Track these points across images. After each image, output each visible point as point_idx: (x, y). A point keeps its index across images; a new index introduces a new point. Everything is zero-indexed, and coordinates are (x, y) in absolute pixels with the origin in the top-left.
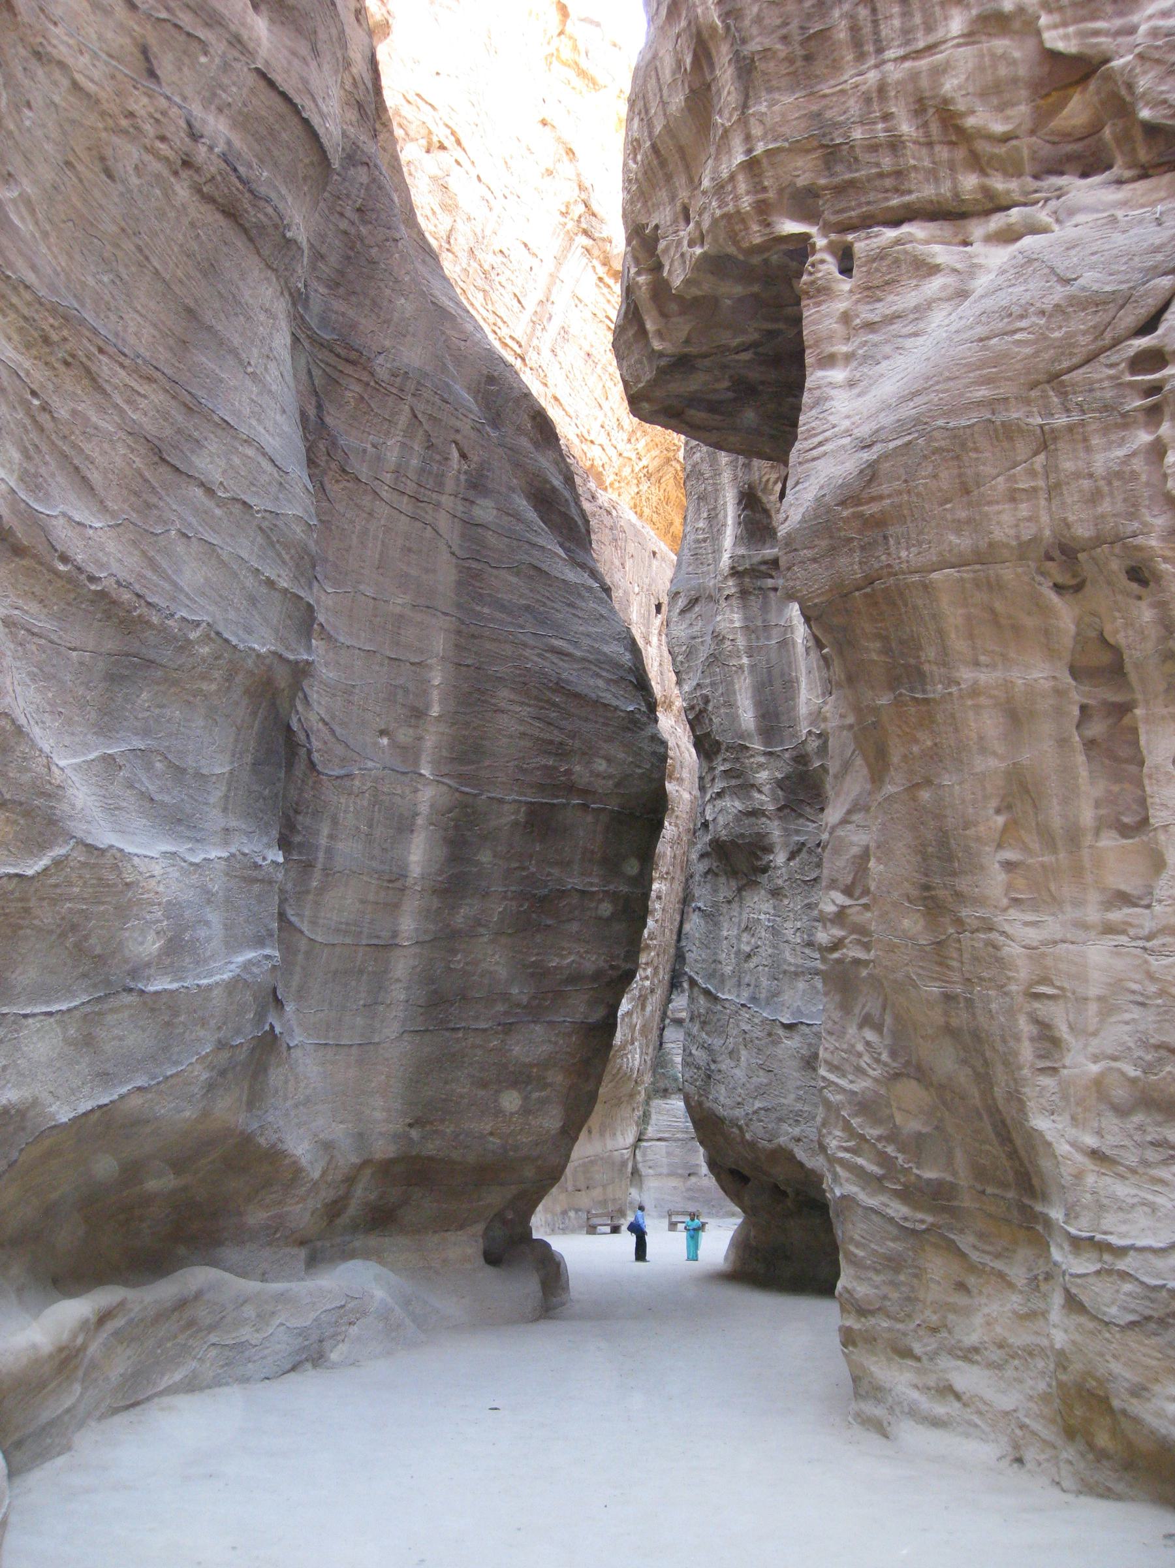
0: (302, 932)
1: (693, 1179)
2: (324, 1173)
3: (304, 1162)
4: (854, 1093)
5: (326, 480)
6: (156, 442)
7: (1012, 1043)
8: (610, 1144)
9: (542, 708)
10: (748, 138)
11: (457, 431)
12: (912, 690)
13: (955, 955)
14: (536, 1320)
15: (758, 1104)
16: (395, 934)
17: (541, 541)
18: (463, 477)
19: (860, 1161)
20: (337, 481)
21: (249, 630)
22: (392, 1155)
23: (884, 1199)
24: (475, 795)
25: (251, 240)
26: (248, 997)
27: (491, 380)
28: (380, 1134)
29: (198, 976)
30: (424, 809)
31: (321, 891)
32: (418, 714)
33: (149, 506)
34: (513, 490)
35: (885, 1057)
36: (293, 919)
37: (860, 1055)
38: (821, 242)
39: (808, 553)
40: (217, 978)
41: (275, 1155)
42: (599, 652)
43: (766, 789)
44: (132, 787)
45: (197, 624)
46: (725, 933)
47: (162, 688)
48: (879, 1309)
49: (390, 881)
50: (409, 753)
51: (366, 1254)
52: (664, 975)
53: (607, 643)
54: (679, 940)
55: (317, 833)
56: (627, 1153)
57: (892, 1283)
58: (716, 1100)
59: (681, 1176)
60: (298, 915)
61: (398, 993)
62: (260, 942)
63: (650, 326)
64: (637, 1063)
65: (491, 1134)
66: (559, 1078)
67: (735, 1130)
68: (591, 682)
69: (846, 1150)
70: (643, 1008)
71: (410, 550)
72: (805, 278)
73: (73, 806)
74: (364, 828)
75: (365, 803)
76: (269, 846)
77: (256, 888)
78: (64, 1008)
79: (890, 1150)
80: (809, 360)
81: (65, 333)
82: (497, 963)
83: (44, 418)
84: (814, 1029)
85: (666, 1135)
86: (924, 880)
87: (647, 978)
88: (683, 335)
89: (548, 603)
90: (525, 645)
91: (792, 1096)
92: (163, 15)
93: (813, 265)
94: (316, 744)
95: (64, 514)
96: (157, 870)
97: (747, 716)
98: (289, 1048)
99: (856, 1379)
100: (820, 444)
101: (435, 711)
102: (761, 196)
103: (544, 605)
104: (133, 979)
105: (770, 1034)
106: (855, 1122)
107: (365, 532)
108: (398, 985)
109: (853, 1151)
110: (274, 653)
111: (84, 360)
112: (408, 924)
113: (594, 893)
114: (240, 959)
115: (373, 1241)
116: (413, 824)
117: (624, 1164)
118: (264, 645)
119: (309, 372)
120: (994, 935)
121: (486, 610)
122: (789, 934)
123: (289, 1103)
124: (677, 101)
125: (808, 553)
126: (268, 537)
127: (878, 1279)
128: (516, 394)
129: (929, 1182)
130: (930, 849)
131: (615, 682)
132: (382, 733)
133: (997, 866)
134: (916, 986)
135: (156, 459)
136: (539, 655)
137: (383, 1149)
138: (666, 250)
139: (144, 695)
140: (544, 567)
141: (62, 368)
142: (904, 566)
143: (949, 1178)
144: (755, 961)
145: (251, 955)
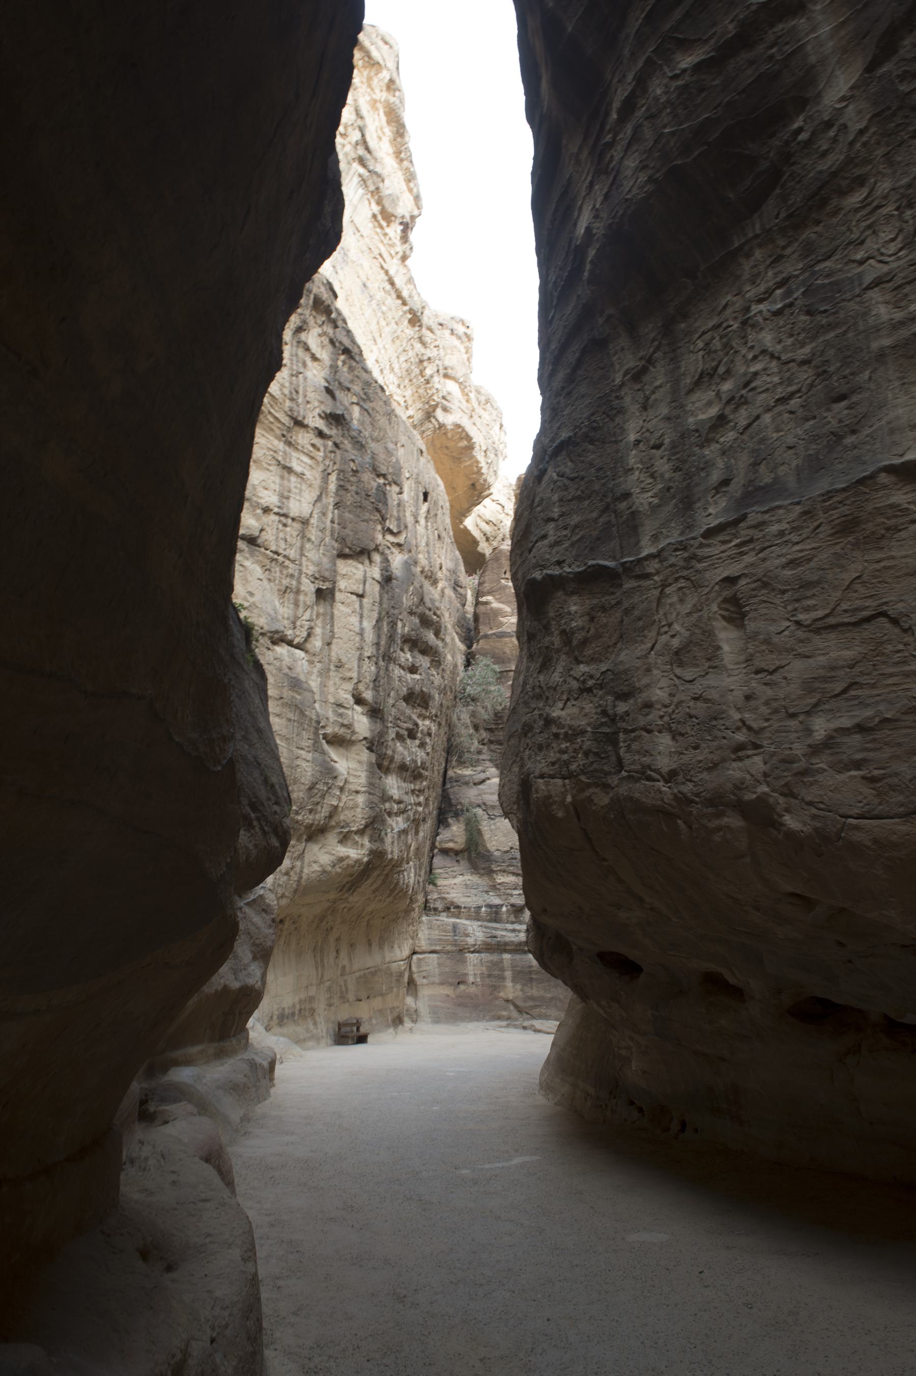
1: (462, 987)
8: (388, 956)
15: (821, 727)
46: (632, 437)
52: (433, 807)
54: (444, 783)
58: (645, 773)
59: (451, 984)
64: (412, 881)
67: (733, 821)
70: (417, 833)
85: (438, 948)
87: (419, 804)
117: (401, 975)
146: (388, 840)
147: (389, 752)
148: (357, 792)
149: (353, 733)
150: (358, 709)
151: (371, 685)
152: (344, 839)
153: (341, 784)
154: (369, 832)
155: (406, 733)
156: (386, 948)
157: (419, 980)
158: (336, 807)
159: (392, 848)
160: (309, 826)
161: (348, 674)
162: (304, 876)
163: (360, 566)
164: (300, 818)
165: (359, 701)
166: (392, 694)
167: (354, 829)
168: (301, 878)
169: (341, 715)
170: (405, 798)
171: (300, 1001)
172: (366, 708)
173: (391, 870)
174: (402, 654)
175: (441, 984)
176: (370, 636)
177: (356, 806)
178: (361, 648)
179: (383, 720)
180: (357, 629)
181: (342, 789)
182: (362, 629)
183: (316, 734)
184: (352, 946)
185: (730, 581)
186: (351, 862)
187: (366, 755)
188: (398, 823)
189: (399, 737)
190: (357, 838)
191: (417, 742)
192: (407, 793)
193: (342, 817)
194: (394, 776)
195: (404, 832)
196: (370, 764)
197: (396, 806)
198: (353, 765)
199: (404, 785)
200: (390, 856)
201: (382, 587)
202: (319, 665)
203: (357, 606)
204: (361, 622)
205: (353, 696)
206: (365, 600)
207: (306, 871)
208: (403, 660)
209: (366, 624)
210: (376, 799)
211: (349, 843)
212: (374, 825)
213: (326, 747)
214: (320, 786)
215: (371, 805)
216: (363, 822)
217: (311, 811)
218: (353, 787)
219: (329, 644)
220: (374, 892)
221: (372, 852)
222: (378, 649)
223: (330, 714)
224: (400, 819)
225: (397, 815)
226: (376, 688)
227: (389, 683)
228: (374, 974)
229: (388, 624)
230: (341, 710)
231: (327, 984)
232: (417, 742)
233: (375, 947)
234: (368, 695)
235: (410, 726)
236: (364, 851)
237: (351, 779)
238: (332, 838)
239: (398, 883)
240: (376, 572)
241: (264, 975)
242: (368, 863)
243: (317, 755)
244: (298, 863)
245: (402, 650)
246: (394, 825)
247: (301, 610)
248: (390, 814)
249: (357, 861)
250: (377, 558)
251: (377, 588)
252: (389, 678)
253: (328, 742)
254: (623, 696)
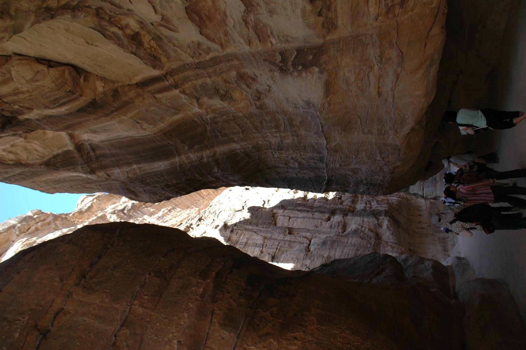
1: (437, 179)
8: (424, 208)
15: (379, 158)
43: (199, 154)
46: (295, 175)
56: (428, 202)
59: (436, 183)
64: (396, 198)
84: (324, 122)
85: (422, 188)
91: (369, 136)
97: (161, 165)
105: (336, 151)
117: (431, 203)
122: (278, 140)
144: (300, 160)
146: (381, 209)
147: (348, 207)
148: (363, 221)
149: (341, 222)
150: (332, 220)
151: (323, 214)
152: (380, 226)
153: (360, 227)
154: (378, 217)
157: (434, 196)
158: (369, 229)
159: (384, 207)
160: (376, 239)
161: (320, 223)
162: (394, 241)
163: (279, 217)
164: (373, 243)
165: (329, 219)
167: (377, 222)
168: (394, 243)
169: (335, 226)
170: (364, 201)
171: (440, 243)
172: (332, 216)
175: (435, 187)
176: (305, 214)
177: (368, 221)
178: (309, 218)
180: (303, 219)
181: (362, 227)
182: (302, 217)
183: (342, 236)
184: (420, 222)
185: (340, 165)
187: (349, 217)
188: (374, 205)
189: (341, 203)
190: (380, 221)
192: (363, 201)
193: (372, 227)
194: (357, 205)
195: (377, 201)
196: (353, 215)
197: (368, 205)
198: (353, 222)
199: (359, 202)
201: (286, 209)
202: (316, 234)
203: (294, 219)
204: (300, 218)
205: (327, 221)
206: (291, 216)
207: (392, 241)
209: (300, 216)
211: (382, 224)
212: (375, 214)
213: (346, 232)
214: (361, 235)
215: (368, 215)
217: (370, 239)
218: (361, 222)
219: (308, 230)
220: (400, 214)
221: (385, 216)
222: (309, 211)
223: (334, 230)
224: (373, 204)
225: (371, 205)
226: (324, 213)
230: (333, 226)
231: (434, 232)
234: (327, 216)
236: (385, 218)
237: (358, 223)
238: (380, 231)
239: (397, 205)
240: (281, 211)
241: (429, 260)
242: (389, 217)
243: (350, 236)
244: (389, 244)
247: (297, 240)
248: (371, 208)
250: (275, 211)
251: (286, 211)
252: (319, 207)
253: (345, 231)
254: (362, 181)
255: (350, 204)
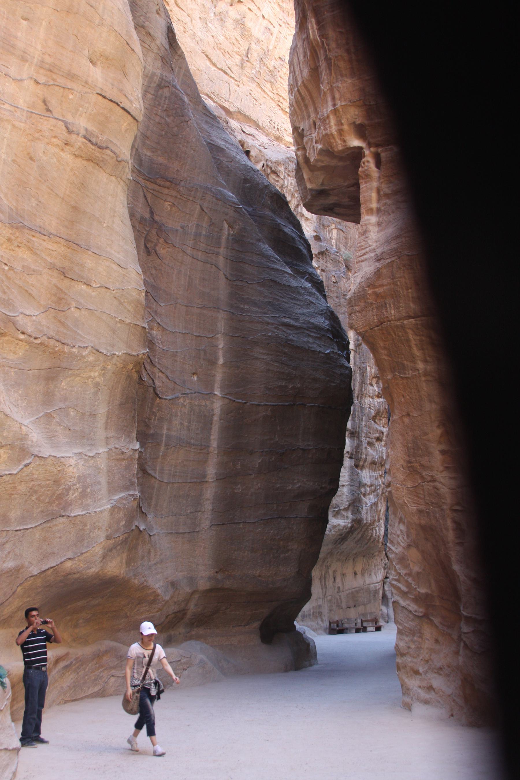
0: (156, 478)
2: (172, 597)
3: (159, 591)
4: (397, 554)
5: (157, 248)
6: (62, 270)
7: (445, 532)
8: (368, 580)
9: (278, 355)
10: (333, 99)
11: (227, 214)
12: (399, 373)
13: (422, 492)
14: (286, 670)
16: (204, 476)
17: (276, 266)
18: (230, 238)
19: (399, 585)
20: (164, 249)
21: (113, 346)
22: (208, 588)
23: (408, 602)
24: (245, 403)
25: (101, 167)
26: (121, 514)
27: (246, 181)
28: (202, 577)
29: (95, 507)
30: (217, 411)
31: (165, 456)
32: (213, 363)
33: (60, 299)
34: (259, 240)
35: (405, 538)
36: (150, 472)
37: (398, 536)
38: (367, 152)
39: (357, 308)
40: (105, 507)
41: (143, 588)
42: (309, 322)
44: (60, 425)
45: (87, 347)
47: (71, 379)
48: (407, 653)
49: (201, 449)
50: (209, 383)
51: (198, 638)
53: (315, 317)
55: (162, 428)
56: (379, 586)
57: (412, 640)
60: (153, 470)
61: (208, 506)
62: (128, 488)
63: (305, 176)
65: (260, 576)
66: (296, 546)
68: (305, 339)
69: (396, 580)
71: (204, 279)
72: (360, 169)
73: (32, 441)
74: (185, 424)
75: (186, 411)
76: (130, 442)
77: (124, 463)
78: (33, 526)
79: (410, 580)
80: (363, 210)
81: (17, 234)
82: (259, 489)
83: (11, 274)
86: (408, 459)
88: (321, 181)
89: (281, 299)
90: (268, 323)
92: (52, 83)
93: (364, 163)
94: (158, 383)
95: (22, 313)
96: (72, 462)
98: (150, 536)
99: (402, 685)
100: (364, 254)
101: (221, 361)
102: (340, 127)
103: (278, 300)
104: (64, 511)
106: (398, 567)
107: (180, 272)
108: (208, 502)
109: (398, 581)
110: (126, 354)
111: (27, 243)
112: (211, 471)
113: (310, 449)
114: (116, 497)
115: (201, 631)
116: (212, 420)
117: (376, 592)
118: (120, 351)
119: (145, 196)
120: (437, 484)
121: (246, 307)
123: (151, 563)
124: (306, 72)
125: (357, 308)
126: (120, 301)
127: (407, 639)
128: (261, 186)
129: (422, 594)
130: (410, 445)
131: (319, 338)
132: (194, 374)
133: (438, 452)
134: (407, 506)
135: (62, 277)
136: (276, 328)
137: (203, 585)
138: (307, 143)
139: (64, 384)
140: (278, 280)
141: (17, 249)
142: (393, 317)
143: (430, 592)
145: (122, 495)
146: (364, 512)
154: (351, 508)
155: (374, 440)
156: (366, 575)
159: (366, 516)
166: (364, 418)
170: (376, 482)
171: (313, 608)
173: (367, 529)
174: (371, 387)
179: (358, 438)
186: (341, 528)
188: (369, 500)
189: (370, 444)
190: (344, 513)
191: (383, 443)
194: (367, 470)
195: (376, 504)
197: (368, 489)
199: (374, 474)
200: (365, 521)
208: (371, 392)
210: (355, 489)
211: (339, 517)
215: (352, 493)
216: (347, 503)
221: (353, 520)
224: (371, 496)
225: (369, 494)
227: (362, 412)
228: (357, 592)
229: (360, 374)
231: (329, 598)
232: (383, 443)
233: (359, 576)
235: (378, 435)
239: (372, 536)
242: (352, 527)
245: (371, 384)
246: (368, 501)
248: (364, 495)
249: (344, 526)
255: (369, 459)
